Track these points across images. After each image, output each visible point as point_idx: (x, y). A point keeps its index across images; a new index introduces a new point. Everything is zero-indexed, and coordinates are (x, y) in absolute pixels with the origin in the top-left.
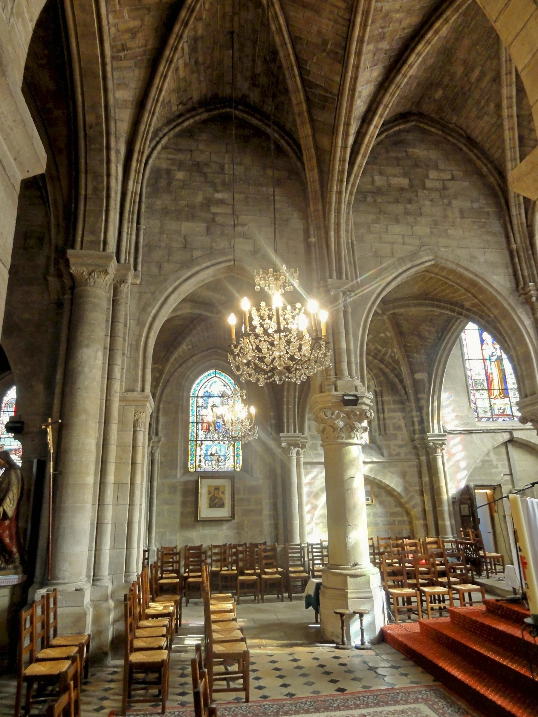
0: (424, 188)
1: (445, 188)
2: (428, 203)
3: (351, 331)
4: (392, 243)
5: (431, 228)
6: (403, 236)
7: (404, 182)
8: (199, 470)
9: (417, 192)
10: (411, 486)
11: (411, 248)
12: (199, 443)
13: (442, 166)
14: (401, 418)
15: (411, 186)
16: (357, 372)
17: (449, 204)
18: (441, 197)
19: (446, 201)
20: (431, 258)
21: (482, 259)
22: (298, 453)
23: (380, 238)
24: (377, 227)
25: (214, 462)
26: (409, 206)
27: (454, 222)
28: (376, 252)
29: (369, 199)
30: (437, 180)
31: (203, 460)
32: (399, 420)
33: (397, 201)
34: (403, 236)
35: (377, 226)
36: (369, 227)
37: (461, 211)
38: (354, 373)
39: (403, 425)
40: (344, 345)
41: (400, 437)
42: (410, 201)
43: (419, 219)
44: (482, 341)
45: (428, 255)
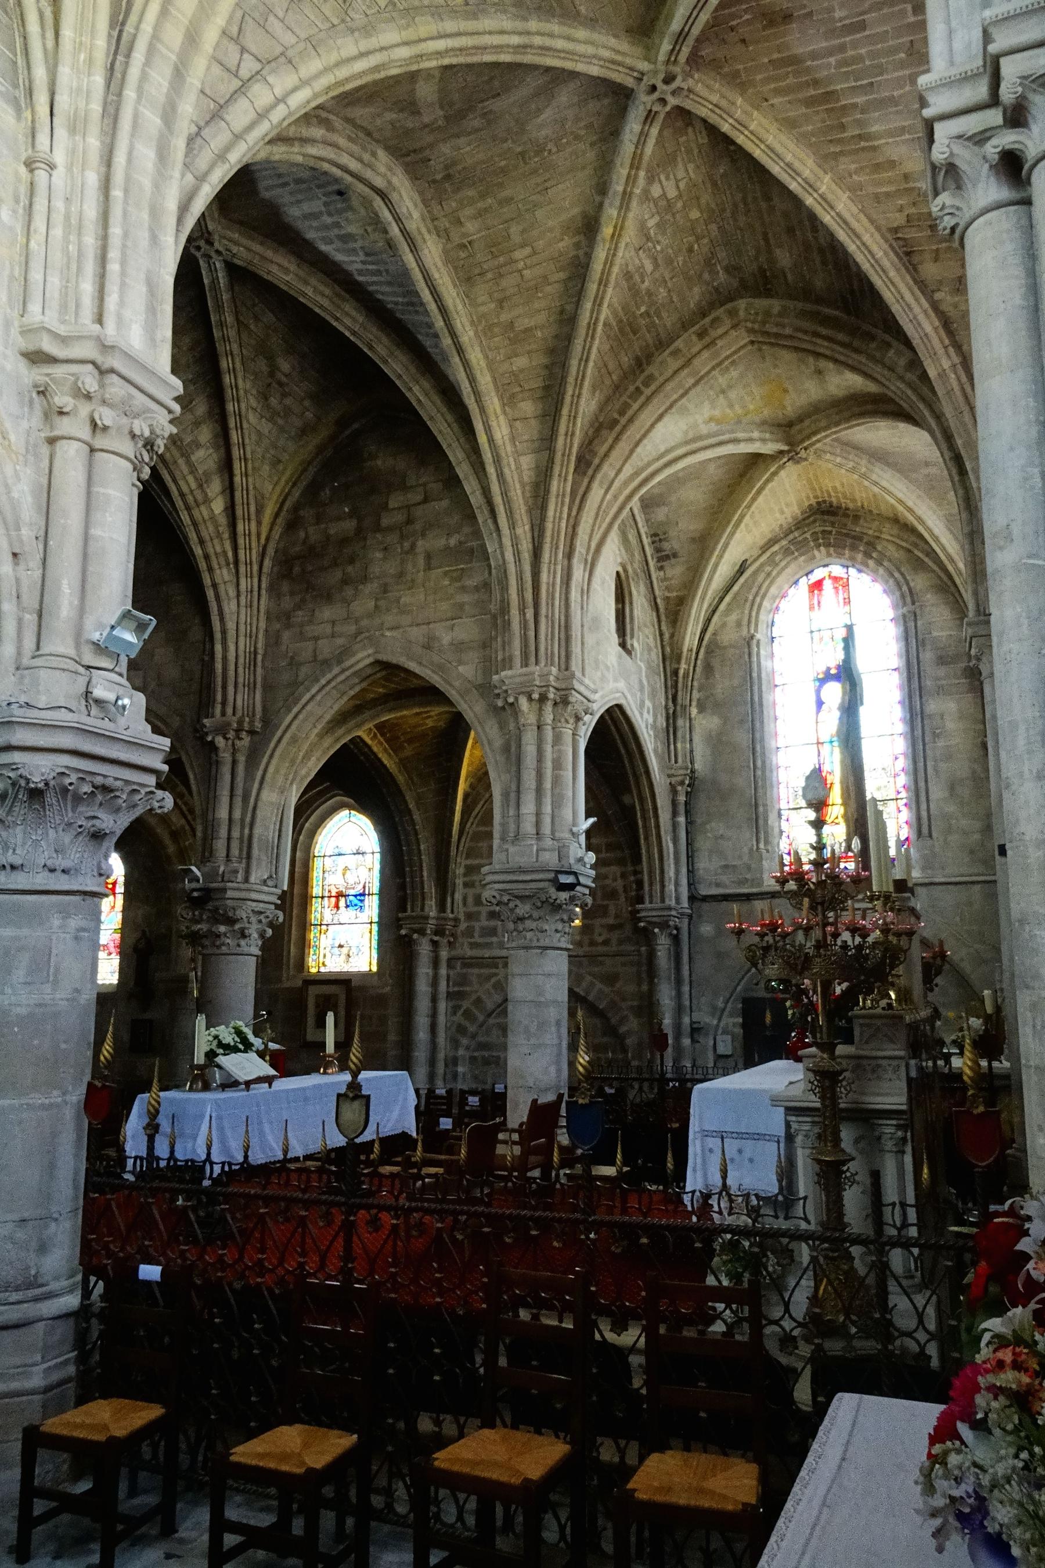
0: (378, 528)
1: (409, 521)
2: (379, 555)
3: (239, 791)
4: (316, 639)
5: (377, 599)
6: (334, 623)
7: (349, 525)
8: (322, 970)
9: (365, 539)
10: (624, 1000)
11: (340, 641)
12: (324, 927)
13: (411, 481)
14: (618, 874)
15: (359, 530)
16: (241, 850)
17: (413, 546)
18: (402, 537)
19: (407, 545)
20: (370, 651)
21: (446, 639)
22: (435, 944)
23: (301, 633)
24: (300, 616)
25: (343, 957)
26: (350, 569)
27: (413, 581)
28: (292, 658)
29: (297, 569)
30: (399, 508)
31: (328, 955)
32: (615, 880)
33: (335, 564)
34: (334, 623)
35: (300, 613)
36: (288, 618)
37: (428, 557)
38: (235, 851)
39: (621, 890)
40: (223, 813)
41: (612, 910)
42: (352, 561)
43: (361, 587)
44: (820, 704)
45: (364, 648)
